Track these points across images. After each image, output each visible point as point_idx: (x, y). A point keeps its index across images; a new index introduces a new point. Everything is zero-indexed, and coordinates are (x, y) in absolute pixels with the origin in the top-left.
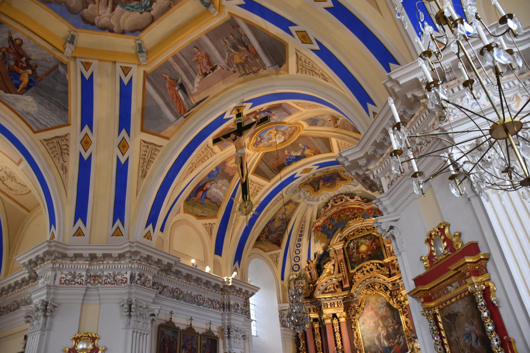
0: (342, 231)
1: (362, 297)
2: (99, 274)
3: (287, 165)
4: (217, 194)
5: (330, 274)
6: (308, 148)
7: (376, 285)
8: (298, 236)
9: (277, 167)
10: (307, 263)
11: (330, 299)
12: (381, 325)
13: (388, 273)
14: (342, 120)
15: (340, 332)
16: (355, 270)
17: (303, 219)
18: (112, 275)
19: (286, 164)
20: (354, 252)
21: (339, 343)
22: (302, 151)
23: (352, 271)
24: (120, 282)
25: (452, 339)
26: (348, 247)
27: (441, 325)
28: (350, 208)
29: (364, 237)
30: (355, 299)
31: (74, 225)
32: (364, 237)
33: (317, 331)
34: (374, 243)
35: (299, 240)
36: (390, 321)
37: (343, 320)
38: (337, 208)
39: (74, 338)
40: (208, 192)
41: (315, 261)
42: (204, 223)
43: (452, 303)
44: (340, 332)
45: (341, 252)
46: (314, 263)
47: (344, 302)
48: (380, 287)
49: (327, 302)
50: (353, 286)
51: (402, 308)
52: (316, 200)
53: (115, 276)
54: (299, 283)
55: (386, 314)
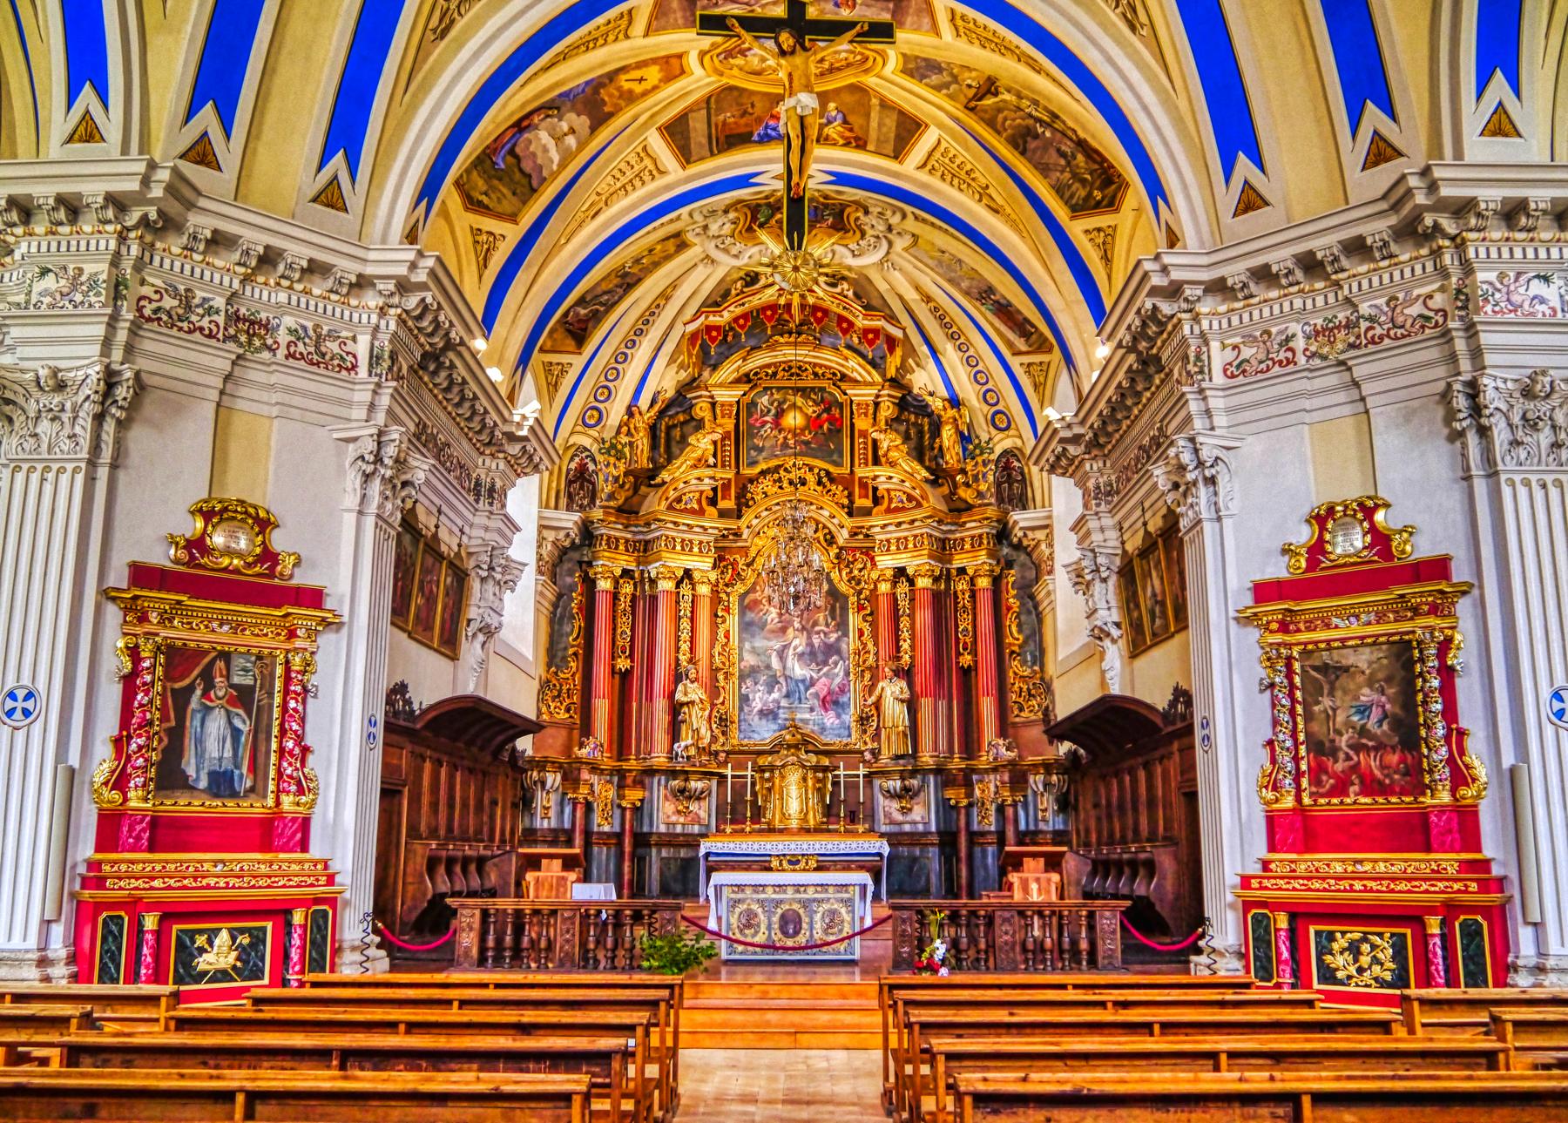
2: (263, 315)
4: (545, 150)
5: (700, 462)
12: (797, 625)
13: (846, 502)
14: (1004, 101)
15: (692, 620)
18: (311, 333)
21: (685, 647)
24: (336, 362)
25: (1316, 708)
26: (753, 404)
27: (1297, 680)
31: (187, 121)
32: (804, 392)
33: (624, 603)
37: (704, 590)
39: (200, 511)
40: (526, 135)
42: (475, 226)
43: (1345, 647)
44: (692, 620)
49: (674, 534)
53: (319, 336)
54: (607, 466)
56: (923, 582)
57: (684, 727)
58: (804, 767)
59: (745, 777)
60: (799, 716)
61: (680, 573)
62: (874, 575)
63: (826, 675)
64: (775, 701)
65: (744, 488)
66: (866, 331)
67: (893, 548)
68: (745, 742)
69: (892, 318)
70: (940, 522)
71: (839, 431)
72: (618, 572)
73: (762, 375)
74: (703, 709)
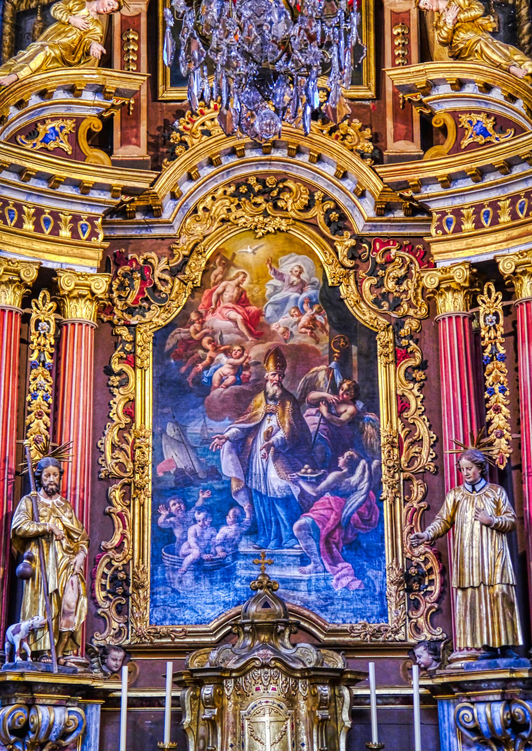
1: (199, 229)
11: (43, 186)
12: (272, 389)
13: (368, 147)
30: (157, 232)
36: (322, 375)
48: (307, 208)
51: (395, 333)
55: (308, 341)
57: (29, 588)
58: (289, 672)
59: (159, 702)
60: (275, 572)
63: (334, 489)
64: (226, 541)
65: (168, 127)
67: (468, 226)
68: (163, 629)
74: (72, 551)
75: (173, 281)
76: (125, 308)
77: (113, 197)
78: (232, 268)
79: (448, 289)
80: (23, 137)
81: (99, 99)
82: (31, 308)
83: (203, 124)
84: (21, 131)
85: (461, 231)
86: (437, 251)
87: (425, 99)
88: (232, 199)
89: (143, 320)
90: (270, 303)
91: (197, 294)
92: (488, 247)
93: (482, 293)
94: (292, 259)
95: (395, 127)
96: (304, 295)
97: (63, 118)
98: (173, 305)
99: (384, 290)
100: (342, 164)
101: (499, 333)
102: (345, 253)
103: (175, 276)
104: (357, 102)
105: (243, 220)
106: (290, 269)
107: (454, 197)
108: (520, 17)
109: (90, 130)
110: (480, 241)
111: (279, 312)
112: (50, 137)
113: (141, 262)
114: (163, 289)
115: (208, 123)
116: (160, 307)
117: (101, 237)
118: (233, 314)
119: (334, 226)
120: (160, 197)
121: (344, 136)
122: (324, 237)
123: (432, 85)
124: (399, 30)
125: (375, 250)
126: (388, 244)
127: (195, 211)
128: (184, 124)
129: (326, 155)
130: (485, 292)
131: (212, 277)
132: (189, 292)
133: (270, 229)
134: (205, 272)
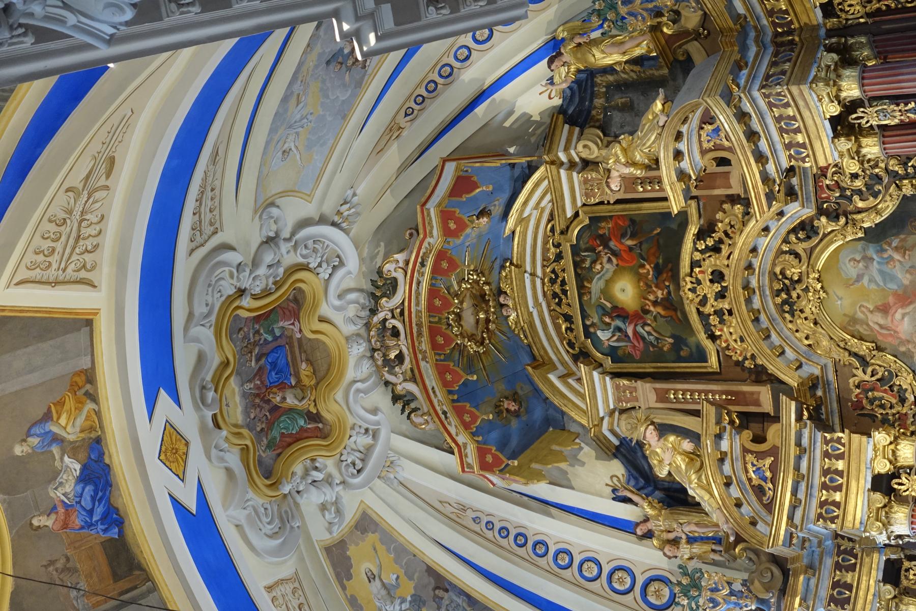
0: (541, 363)
1: (825, 343)
3: (121, 533)
6: (47, 417)
7: (782, 272)
8: (521, 551)
9: (116, 577)
10: (646, 542)
11: (803, 486)
16: (708, 344)
17: (448, 510)
19: (114, 533)
20: (635, 332)
22: (55, 450)
23: (713, 361)
26: (613, 353)
28: (431, 308)
29: (582, 280)
30: (831, 376)
32: (582, 280)
34: (612, 244)
35: (541, 550)
38: (424, 358)
41: (645, 505)
45: (626, 388)
46: (650, 512)
47: (837, 427)
48: (797, 256)
49: (815, 503)
50: (771, 369)
52: (368, 440)
56: (851, 90)
61: (879, 499)
62: (853, 167)
66: (447, 233)
69: (423, 190)
70: (739, 66)
71: (633, 221)
72: (888, 590)
73: (571, 336)
75: (873, 364)
76: (900, 404)
77: (805, 426)
78: (856, 316)
79: (858, 152)
80: (765, 498)
81: (726, 436)
82: (907, 495)
83: (735, 341)
84: (761, 501)
85: (804, 143)
86: (824, 161)
87: (694, 177)
88: (796, 317)
89: (910, 390)
90: (885, 284)
91: (883, 346)
92: (817, 122)
93: (859, 124)
94: (844, 267)
95: (719, 188)
96: (875, 257)
97: (745, 463)
98: (894, 367)
99: (864, 189)
100: (755, 233)
101: (896, 108)
102: (834, 224)
103: (868, 363)
104: (702, 212)
105: (813, 309)
106: (853, 270)
107: (775, 151)
108: (616, 81)
109: (752, 441)
110: (812, 129)
111: (893, 278)
112: (761, 475)
113: (858, 391)
114: (880, 374)
115: (734, 337)
116: (897, 376)
117: (840, 435)
118: (898, 316)
119: (811, 234)
120: (801, 380)
121: (732, 226)
122: (821, 240)
123: (682, 176)
124: (639, 187)
125: (828, 198)
126: (821, 187)
127: (810, 345)
128: (737, 355)
129: (750, 247)
130: (859, 121)
131: (865, 333)
132: (881, 354)
133: (819, 286)
134: (861, 339)
